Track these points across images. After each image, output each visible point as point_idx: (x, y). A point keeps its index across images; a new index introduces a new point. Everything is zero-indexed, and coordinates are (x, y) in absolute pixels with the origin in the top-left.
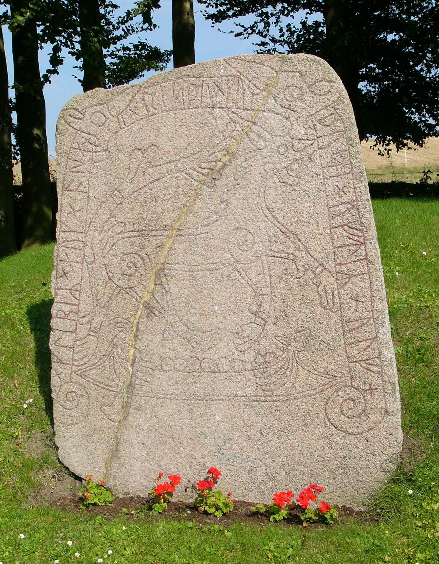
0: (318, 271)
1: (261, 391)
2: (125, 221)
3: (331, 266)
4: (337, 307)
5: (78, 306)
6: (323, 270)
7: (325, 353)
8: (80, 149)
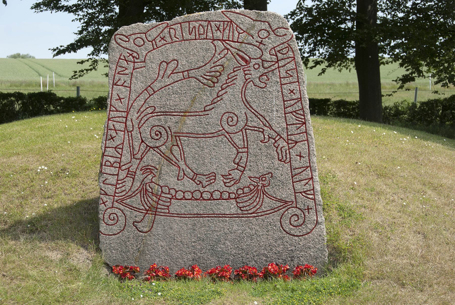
0: (277, 139)
1: (240, 211)
2: (155, 106)
3: (285, 136)
4: (288, 160)
5: (121, 158)
6: (280, 138)
7: (280, 188)
8: (126, 60)
